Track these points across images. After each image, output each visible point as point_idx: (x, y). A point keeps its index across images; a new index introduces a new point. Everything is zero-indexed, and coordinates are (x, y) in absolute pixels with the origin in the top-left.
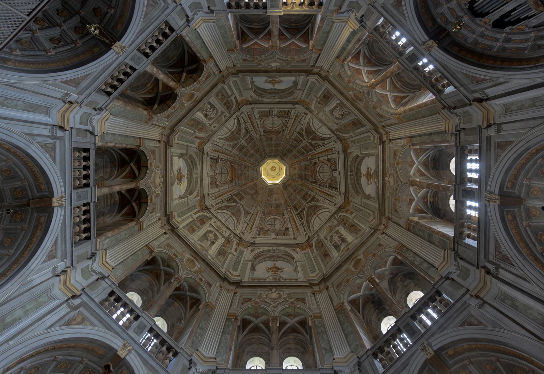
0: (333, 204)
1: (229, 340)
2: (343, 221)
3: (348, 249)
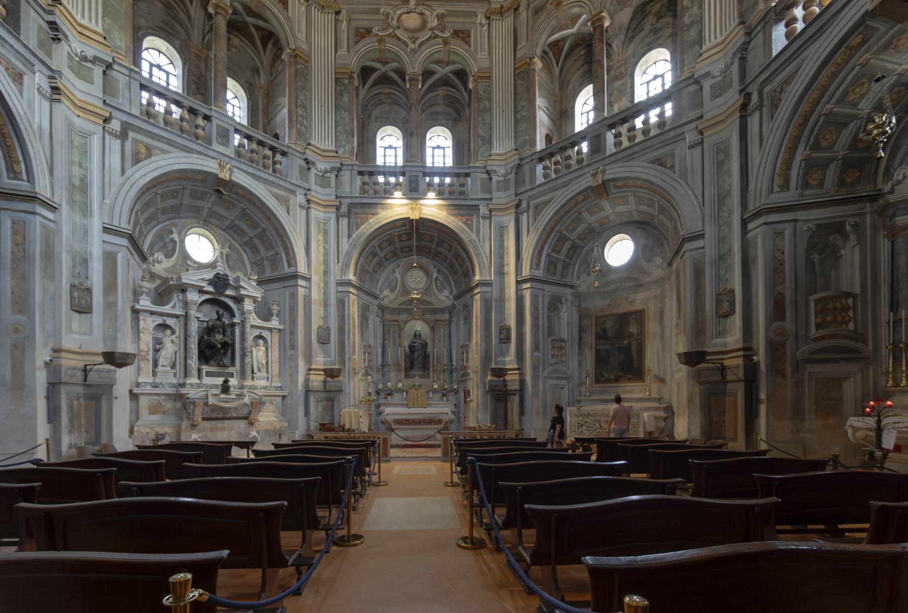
1: (347, 120)
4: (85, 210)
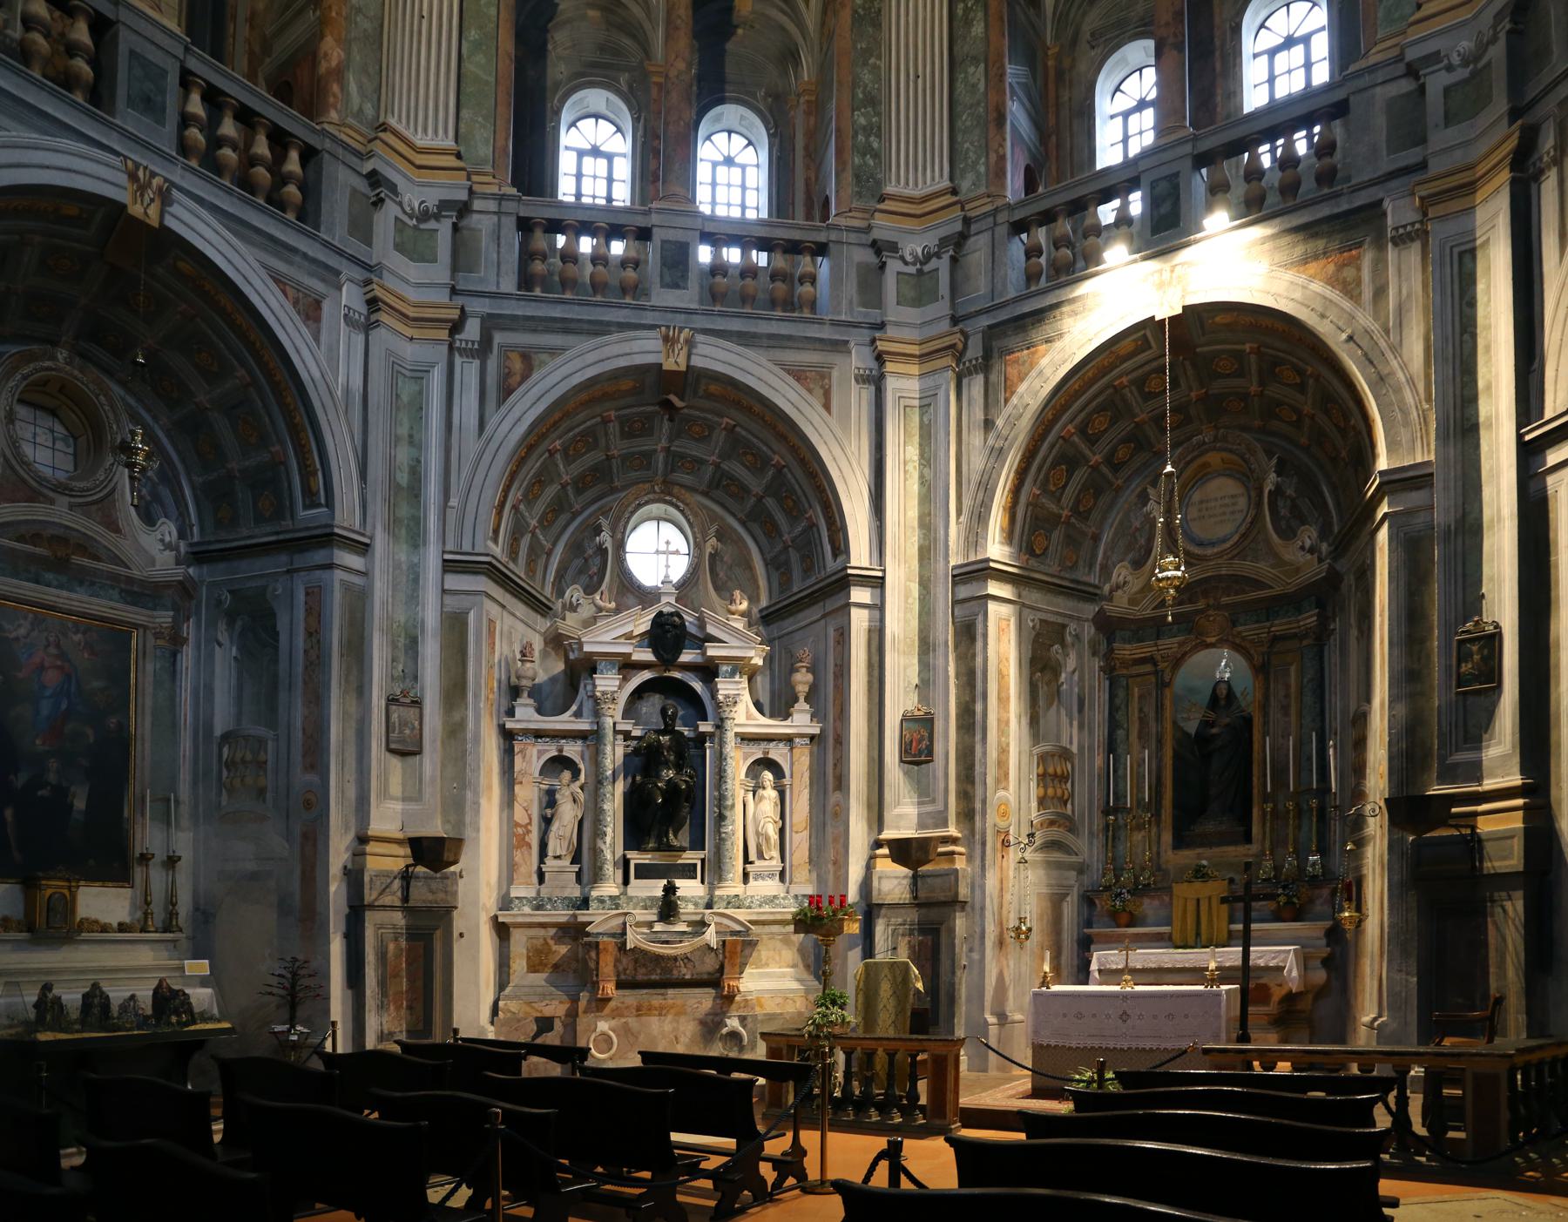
1: (982, 87)
4: (416, 539)
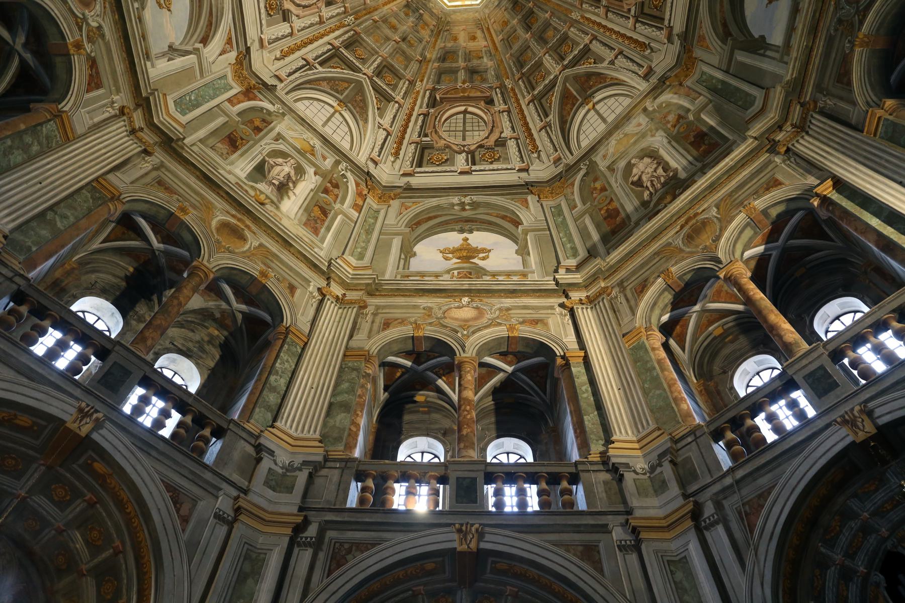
0: (375, 155)
2: (331, 186)
3: (262, 204)
